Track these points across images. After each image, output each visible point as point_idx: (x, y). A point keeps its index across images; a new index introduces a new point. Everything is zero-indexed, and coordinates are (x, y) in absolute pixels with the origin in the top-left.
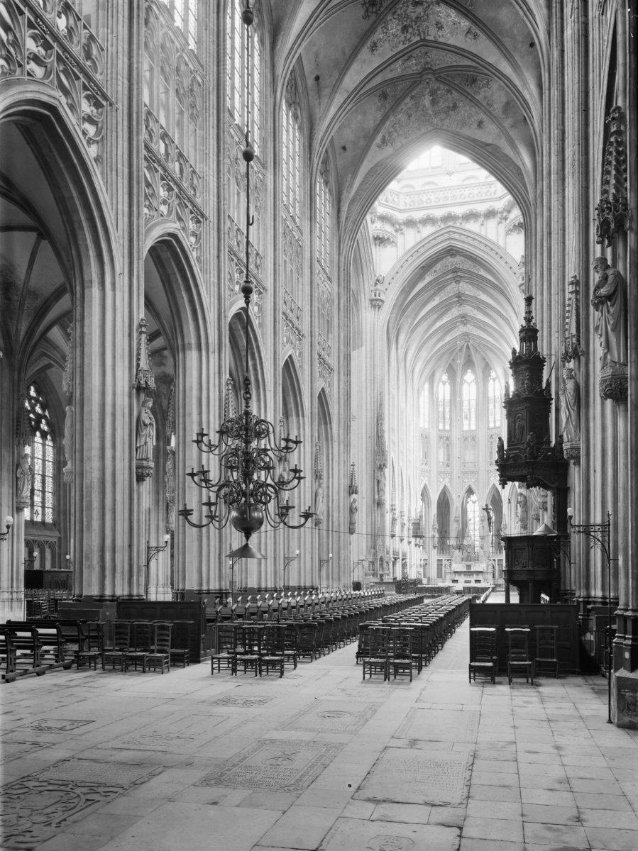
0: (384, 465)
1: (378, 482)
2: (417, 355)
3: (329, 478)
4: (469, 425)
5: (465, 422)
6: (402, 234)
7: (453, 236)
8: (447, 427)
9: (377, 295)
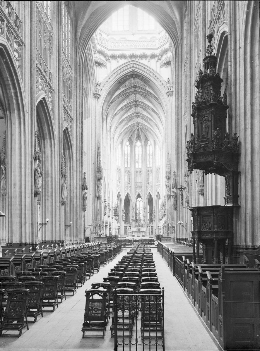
0: (101, 178)
1: (98, 187)
2: (115, 130)
3: (71, 180)
4: (139, 166)
5: (137, 164)
6: (110, 62)
7: (135, 66)
8: (129, 166)
9: (97, 91)
